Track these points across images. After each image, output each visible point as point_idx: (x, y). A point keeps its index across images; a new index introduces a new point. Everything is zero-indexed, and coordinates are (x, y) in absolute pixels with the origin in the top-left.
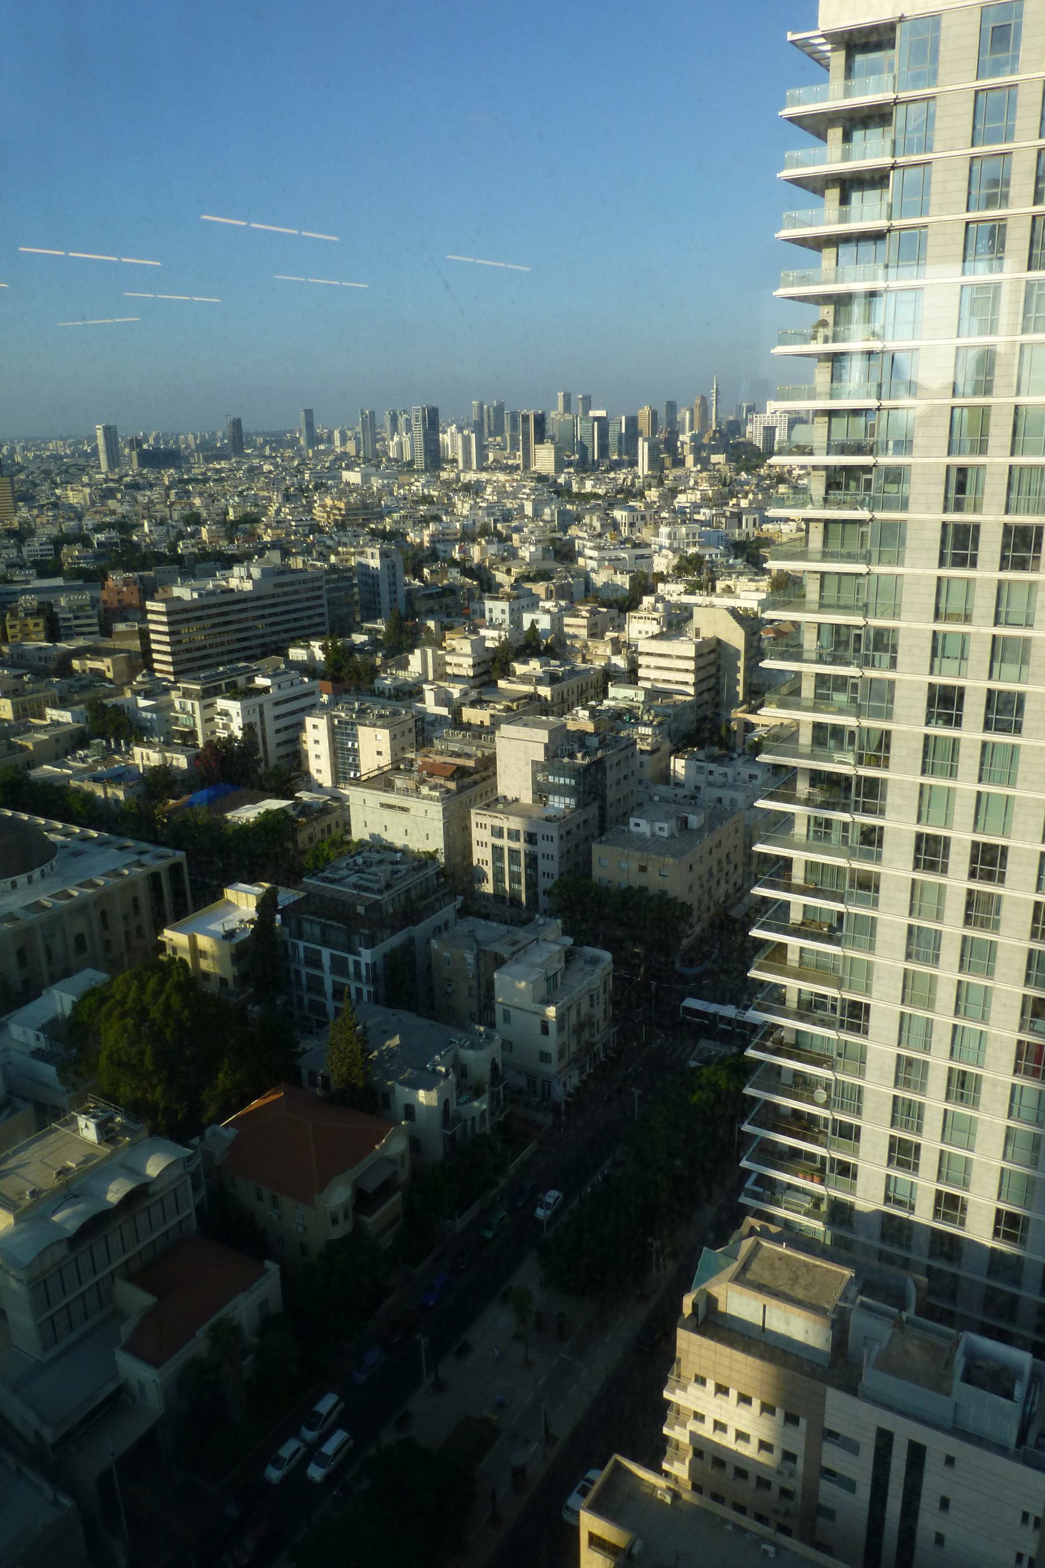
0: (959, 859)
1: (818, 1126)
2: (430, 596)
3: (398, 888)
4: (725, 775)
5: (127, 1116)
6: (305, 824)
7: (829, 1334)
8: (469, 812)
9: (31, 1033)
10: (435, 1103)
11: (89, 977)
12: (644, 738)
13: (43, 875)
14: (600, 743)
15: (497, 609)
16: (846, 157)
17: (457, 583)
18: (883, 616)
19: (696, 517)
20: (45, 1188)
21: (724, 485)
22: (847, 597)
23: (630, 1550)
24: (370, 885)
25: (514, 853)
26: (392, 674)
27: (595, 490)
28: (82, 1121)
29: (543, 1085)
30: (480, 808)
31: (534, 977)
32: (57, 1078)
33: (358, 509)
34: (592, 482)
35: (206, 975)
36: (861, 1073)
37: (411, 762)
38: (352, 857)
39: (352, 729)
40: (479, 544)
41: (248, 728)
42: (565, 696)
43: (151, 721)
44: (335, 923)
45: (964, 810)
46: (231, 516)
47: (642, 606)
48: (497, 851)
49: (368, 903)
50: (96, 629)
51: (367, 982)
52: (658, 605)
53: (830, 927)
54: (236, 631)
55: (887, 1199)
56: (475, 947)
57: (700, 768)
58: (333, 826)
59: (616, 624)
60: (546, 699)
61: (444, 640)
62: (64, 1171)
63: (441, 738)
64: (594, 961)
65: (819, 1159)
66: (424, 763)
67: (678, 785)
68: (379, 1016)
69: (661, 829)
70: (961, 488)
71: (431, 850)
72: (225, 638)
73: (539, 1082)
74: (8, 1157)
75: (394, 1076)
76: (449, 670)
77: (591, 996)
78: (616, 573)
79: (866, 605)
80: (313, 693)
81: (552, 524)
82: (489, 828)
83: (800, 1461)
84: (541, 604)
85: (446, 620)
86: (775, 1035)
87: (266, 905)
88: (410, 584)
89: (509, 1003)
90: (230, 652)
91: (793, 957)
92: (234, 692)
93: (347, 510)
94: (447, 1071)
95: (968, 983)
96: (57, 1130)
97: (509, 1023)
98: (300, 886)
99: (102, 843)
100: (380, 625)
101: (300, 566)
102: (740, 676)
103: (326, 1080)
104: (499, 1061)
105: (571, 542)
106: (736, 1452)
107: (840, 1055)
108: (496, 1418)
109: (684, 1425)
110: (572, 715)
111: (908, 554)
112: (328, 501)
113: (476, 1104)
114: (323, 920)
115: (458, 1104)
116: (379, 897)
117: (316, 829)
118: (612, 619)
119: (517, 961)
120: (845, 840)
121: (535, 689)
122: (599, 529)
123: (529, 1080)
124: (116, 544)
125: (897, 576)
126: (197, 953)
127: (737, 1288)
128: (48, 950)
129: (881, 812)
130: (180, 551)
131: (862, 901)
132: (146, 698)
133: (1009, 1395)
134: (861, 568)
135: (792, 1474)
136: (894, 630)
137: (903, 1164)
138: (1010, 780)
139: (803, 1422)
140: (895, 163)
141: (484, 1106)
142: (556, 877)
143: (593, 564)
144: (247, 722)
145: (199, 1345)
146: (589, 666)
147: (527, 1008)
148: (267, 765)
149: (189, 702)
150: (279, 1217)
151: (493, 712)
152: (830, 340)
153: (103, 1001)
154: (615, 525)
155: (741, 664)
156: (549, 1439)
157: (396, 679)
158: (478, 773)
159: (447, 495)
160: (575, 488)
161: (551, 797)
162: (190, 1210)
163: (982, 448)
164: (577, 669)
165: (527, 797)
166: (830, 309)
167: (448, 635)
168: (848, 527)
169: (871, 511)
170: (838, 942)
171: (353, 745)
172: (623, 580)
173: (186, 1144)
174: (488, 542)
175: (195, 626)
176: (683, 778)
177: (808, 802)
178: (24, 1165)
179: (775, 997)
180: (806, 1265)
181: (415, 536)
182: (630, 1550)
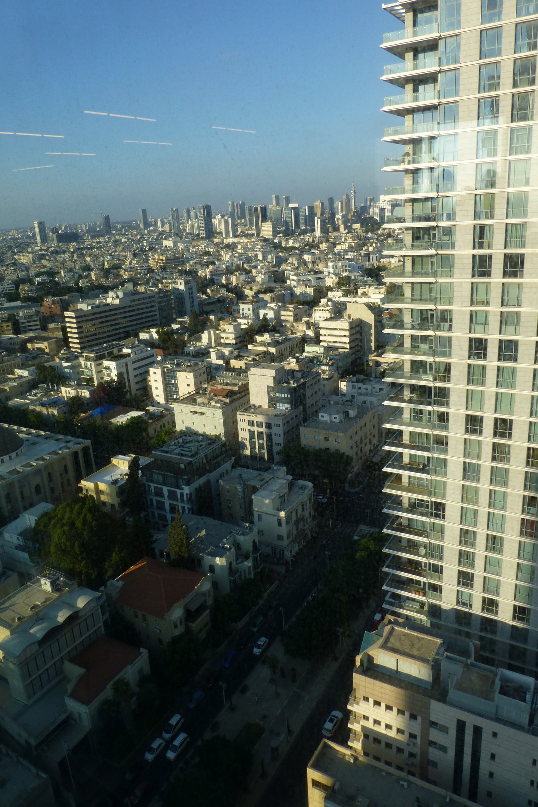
0: (488, 427)
1: (421, 567)
2: (210, 304)
4: (367, 389)
5: (66, 577)
6: (152, 423)
7: (431, 673)
9: (15, 537)
10: (225, 564)
11: (43, 507)
12: (324, 371)
13: (17, 455)
14: (302, 375)
15: (246, 308)
16: (415, 67)
17: (224, 296)
18: (444, 304)
19: (346, 257)
20: (26, 616)
21: (360, 240)
22: (426, 295)
23: (334, 786)
25: (260, 434)
26: (193, 344)
27: (293, 245)
28: (43, 581)
29: (280, 552)
31: (273, 497)
32: (29, 559)
33: (171, 260)
34: (292, 241)
35: (104, 503)
36: (442, 539)
37: (205, 389)
39: (174, 373)
40: (236, 275)
41: (120, 375)
43: (69, 373)
46: (106, 266)
47: (320, 304)
48: (252, 433)
50: (39, 327)
51: (188, 503)
52: (329, 303)
54: (112, 325)
55: (458, 603)
56: (242, 481)
57: (353, 386)
58: (166, 424)
59: (308, 313)
60: (273, 354)
61: (219, 325)
62: (35, 607)
63: (220, 376)
64: (303, 488)
65: (422, 584)
66: (212, 389)
67: (343, 395)
68: (193, 520)
69: (335, 418)
70: (481, 236)
71: (217, 434)
72: (106, 329)
74: (6, 601)
75: (203, 551)
76: (223, 341)
77: (303, 505)
78: (306, 287)
79: (435, 298)
80: (152, 356)
81: (272, 264)
82: (247, 421)
83: (419, 739)
84: (269, 305)
85: (220, 315)
86: (398, 521)
87: (134, 465)
88: (200, 297)
89: (260, 511)
90: (109, 336)
91: (405, 480)
92: (113, 357)
93: (166, 260)
94: (230, 547)
95: (495, 490)
96: (30, 586)
98: (151, 455)
99: (47, 438)
100: (186, 319)
101: (143, 290)
102: (373, 338)
103: (168, 554)
104: (257, 541)
106: (386, 735)
107: (431, 530)
108: (262, 723)
109: (358, 722)
110: (287, 361)
111: (456, 271)
112: (156, 256)
113: (246, 563)
114: (163, 472)
115: (237, 564)
116: (191, 459)
117: (157, 425)
119: (264, 489)
120: (430, 420)
121: (267, 349)
122: (297, 265)
123: (272, 550)
124: (47, 283)
125: (451, 283)
126: (99, 492)
128: (22, 493)
129: (447, 404)
130: (80, 285)
132: (67, 362)
133: (524, 700)
134: (432, 280)
135: (414, 745)
136: (450, 311)
137: (466, 585)
138: (512, 385)
139: (419, 718)
140: (441, 69)
141: (250, 564)
142: (282, 445)
144: (119, 372)
145: (108, 692)
146: (295, 336)
148: (131, 394)
149: (89, 363)
151: (246, 362)
152: (411, 163)
153: (50, 519)
154: (305, 263)
155: (373, 331)
156: (290, 732)
157: (195, 347)
158: (239, 393)
159: (218, 251)
160: (283, 245)
161: (278, 405)
162: (101, 624)
164: (289, 338)
165: (265, 405)
166: (411, 146)
167: (221, 323)
168: (425, 259)
169: (436, 250)
170: (427, 472)
171: (175, 382)
172: (310, 291)
173: (97, 590)
175: (90, 323)
176: (345, 391)
177: (410, 401)
178: (13, 605)
179: (397, 502)
180: (418, 638)
181: (202, 272)
182: (334, 786)
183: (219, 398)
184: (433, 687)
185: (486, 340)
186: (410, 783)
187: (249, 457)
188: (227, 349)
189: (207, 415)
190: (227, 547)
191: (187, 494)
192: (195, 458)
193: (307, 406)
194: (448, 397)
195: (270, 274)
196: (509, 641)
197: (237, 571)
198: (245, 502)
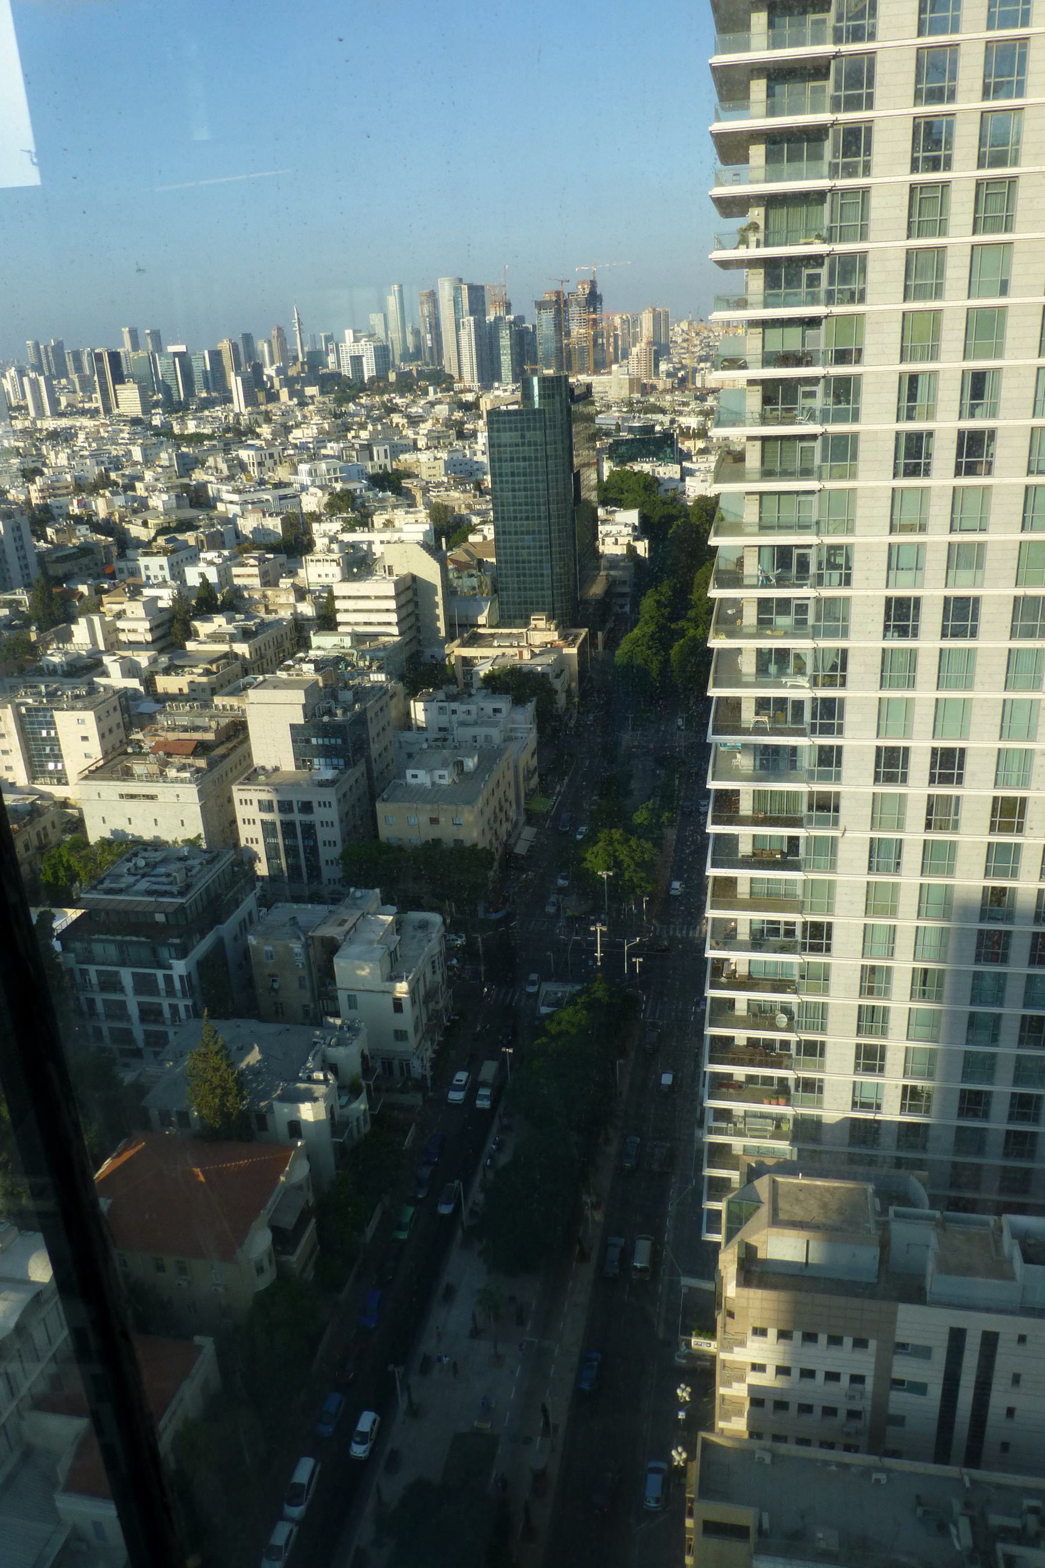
0: (919, 765)
1: (773, 1049)
4: (469, 712)
6: (17, 832)
10: (323, 1115)
15: (154, 566)
17: (90, 540)
18: (835, 532)
19: (323, 451)
21: (336, 416)
22: (789, 515)
24: (167, 888)
26: (58, 648)
27: (198, 430)
29: (401, 1068)
34: (194, 422)
36: (825, 990)
38: (129, 860)
39: (45, 716)
44: (134, 939)
45: (923, 718)
48: (268, 828)
49: (170, 909)
51: (184, 995)
53: (782, 853)
55: (854, 1104)
56: (299, 933)
58: (49, 829)
60: (244, 656)
61: (100, 603)
64: (424, 926)
65: (776, 1082)
67: (420, 728)
69: (441, 777)
70: (912, 396)
73: (396, 1063)
76: (123, 637)
77: (433, 962)
78: (264, 515)
81: (172, 469)
83: (869, 1383)
88: (35, 547)
91: (743, 890)
94: (325, 1076)
97: (356, 1008)
102: (440, 611)
103: (184, 1117)
104: (366, 1052)
105: (203, 486)
109: (741, 1379)
114: (119, 938)
116: (183, 901)
119: (351, 941)
121: (231, 647)
122: (226, 472)
127: (775, 1230)
131: (823, 823)
135: (862, 1394)
137: (869, 1069)
139: (873, 1344)
143: (235, 509)
152: (762, 245)
154: (243, 467)
155: (439, 599)
157: (66, 653)
158: (222, 743)
159: (35, 446)
160: (177, 430)
163: (933, 355)
164: (267, 621)
165: (288, 764)
167: (105, 599)
168: (786, 444)
170: (795, 867)
171: (48, 733)
172: (274, 524)
174: (113, 493)
180: (827, 1189)
183: (184, 761)
184: (878, 1277)
185: (977, 600)
188: (141, 653)
189: (160, 798)
190: (171, 1067)
191: (181, 977)
192: (188, 897)
193: (373, 757)
194: (841, 717)
195: (179, 490)
196: (1000, 1162)
197: (346, 1124)
198: (311, 974)
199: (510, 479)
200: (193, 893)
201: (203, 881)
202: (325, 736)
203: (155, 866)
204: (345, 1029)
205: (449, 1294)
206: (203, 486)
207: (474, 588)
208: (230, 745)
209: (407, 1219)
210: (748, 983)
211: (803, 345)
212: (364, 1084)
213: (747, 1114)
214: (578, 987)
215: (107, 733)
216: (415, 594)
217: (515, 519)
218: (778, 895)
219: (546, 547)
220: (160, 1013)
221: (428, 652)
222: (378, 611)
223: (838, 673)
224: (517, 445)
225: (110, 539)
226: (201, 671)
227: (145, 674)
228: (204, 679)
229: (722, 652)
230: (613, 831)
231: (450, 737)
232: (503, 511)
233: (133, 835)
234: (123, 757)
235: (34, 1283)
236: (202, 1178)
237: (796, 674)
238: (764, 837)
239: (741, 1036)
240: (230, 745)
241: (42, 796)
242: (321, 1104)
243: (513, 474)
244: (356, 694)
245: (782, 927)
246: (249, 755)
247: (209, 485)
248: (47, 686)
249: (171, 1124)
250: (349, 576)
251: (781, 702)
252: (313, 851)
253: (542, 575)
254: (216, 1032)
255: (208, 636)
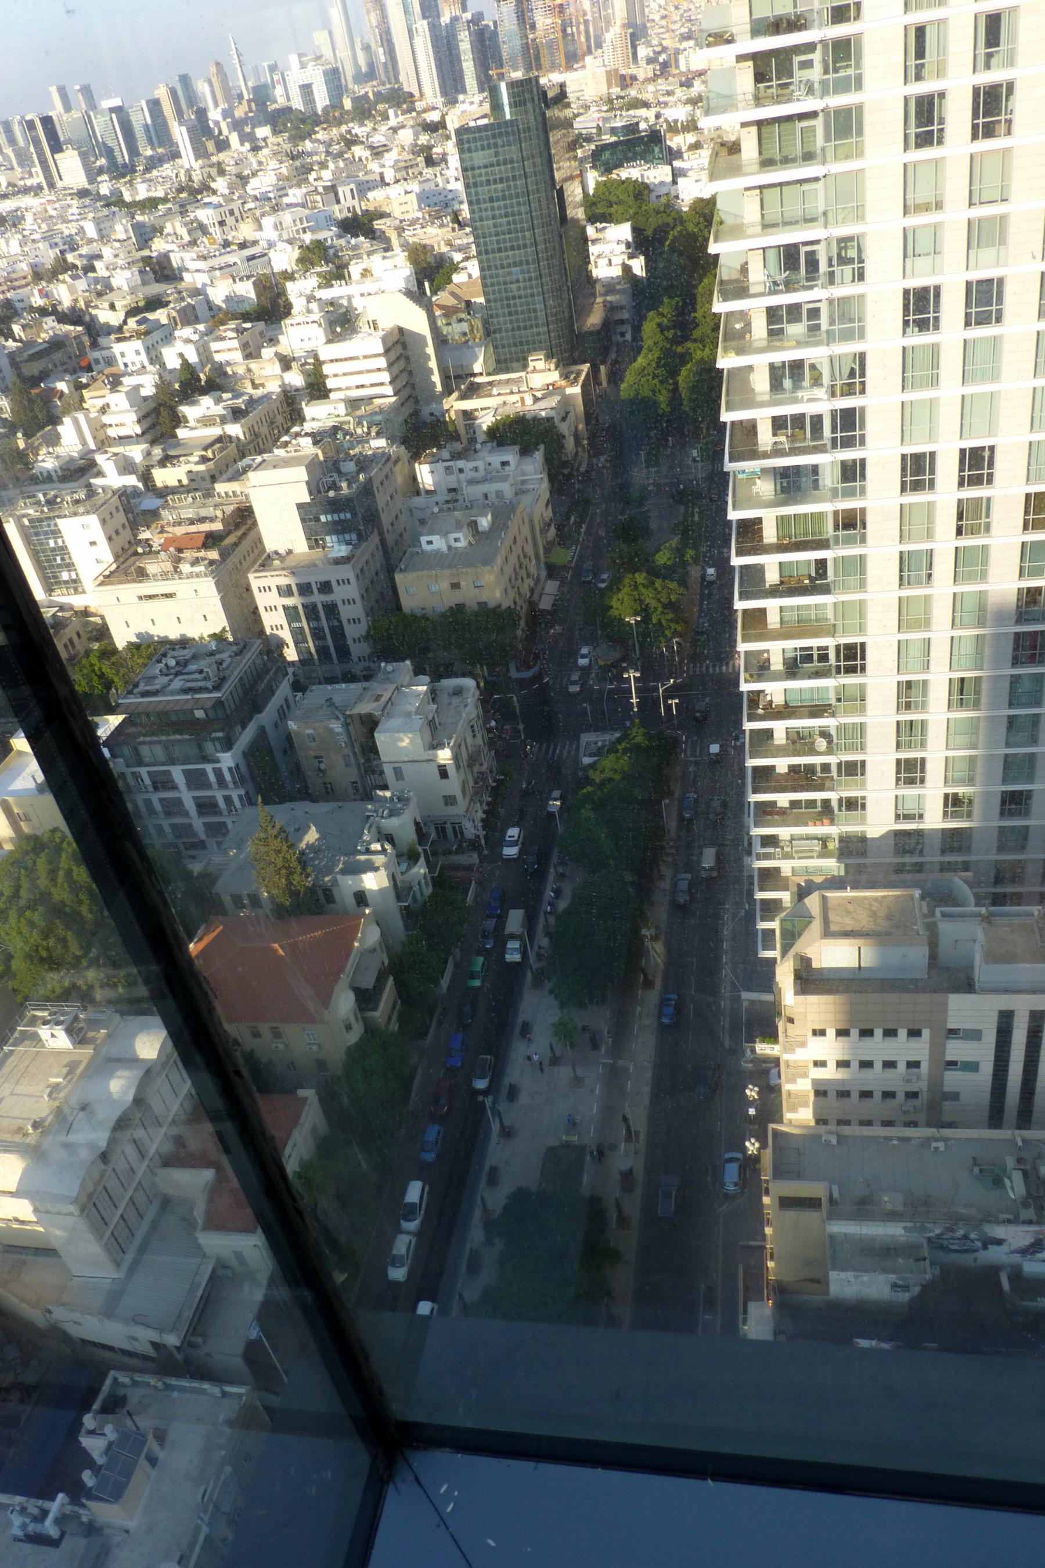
0: (947, 469)
3: (232, 678)
4: (476, 469)
8: (247, 578)
10: (385, 883)
19: (286, 200)
20: (44, 1114)
21: (293, 158)
22: (794, 209)
26: (49, 453)
28: (44, 1032)
29: (454, 829)
30: (256, 571)
34: (145, 186)
36: (863, 710)
38: (159, 661)
39: (49, 526)
42: (256, 430)
44: (178, 737)
48: (291, 613)
51: (236, 786)
53: (810, 577)
55: (897, 817)
56: (337, 713)
57: (447, 468)
60: (238, 438)
61: (82, 400)
64: (458, 692)
65: (819, 804)
67: (428, 492)
69: (456, 540)
70: (920, 53)
71: (217, 631)
73: (449, 827)
76: (112, 432)
77: (472, 727)
78: (234, 281)
81: (129, 242)
82: (274, 590)
83: (925, 1067)
88: (4, 347)
91: (773, 620)
94: (382, 846)
96: (12, 1052)
97: (403, 779)
102: (433, 364)
104: (419, 820)
105: (166, 256)
109: (805, 1075)
114: (163, 738)
118: (261, 333)
119: (390, 716)
122: (187, 238)
131: (849, 541)
135: (919, 1078)
137: (910, 782)
138: (994, 376)
139: (926, 1033)
147: (420, 758)
150: (286, 1046)
154: (203, 229)
155: (430, 350)
157: (57, 457)
158: (229, 533)
160: (127, 197)
165: (300, 545)
167: (85, 393)
168: (784, 126)
170: (826, 590)
172: (247, 290)
174: (74, 277)
180: (875, 899)
184: (929, 973)
186: (945, 1140)
187: (298, 664)
190: (235, 854)
191: (230, 769)
192: (223, 690)
194: (862, 426)
199: (489, 205)
200: (228, 686)
201: (236, 673)
202: (333, 512)
203: (186, 663)
204: (396, 800)
205: (526, 1030)
206: (166, 256)
207: (465, 334)
208: (239, 533)
209: (478, 968)
210: (786, 711)
211: (795, 7)
212: (420, 849)
213: (793, 838)
214: (617, 735)
215: (114, 536)
216: (404, 346)
217: (500, 250)
218: (810, 620)
219: (536, 278)
220: (215, 805)
221: (425, 411)
222: (369, 371)
223: (857, 380)
224: (492, 165)
225: (80, 328)
226: (197, 459)
227: (141, 469)
228: (202, 468)
229: (733, 372)
230: (637, 575)
231: (461, 498)
232: (485, 244)
233: (158, 636)
234: (133, 558)
235: (143, 1060)
236: (281, 952)
237: (812, 386)
238: (791, 563)
239: (782, 764)
240: (239, 533)
241: (62, 608)
242: (383, 873)
243: (491, 200)
244: (358, 462)
245: (815, 653)
246: (260, 540)
247: (171, 255)
248: (45, 495)
249: (243, 906)
250: (333, 338)
251: (798, 420)
252: (338, 632)
253: (535, 311)
254: (272, 817)
255: (198, 421)
